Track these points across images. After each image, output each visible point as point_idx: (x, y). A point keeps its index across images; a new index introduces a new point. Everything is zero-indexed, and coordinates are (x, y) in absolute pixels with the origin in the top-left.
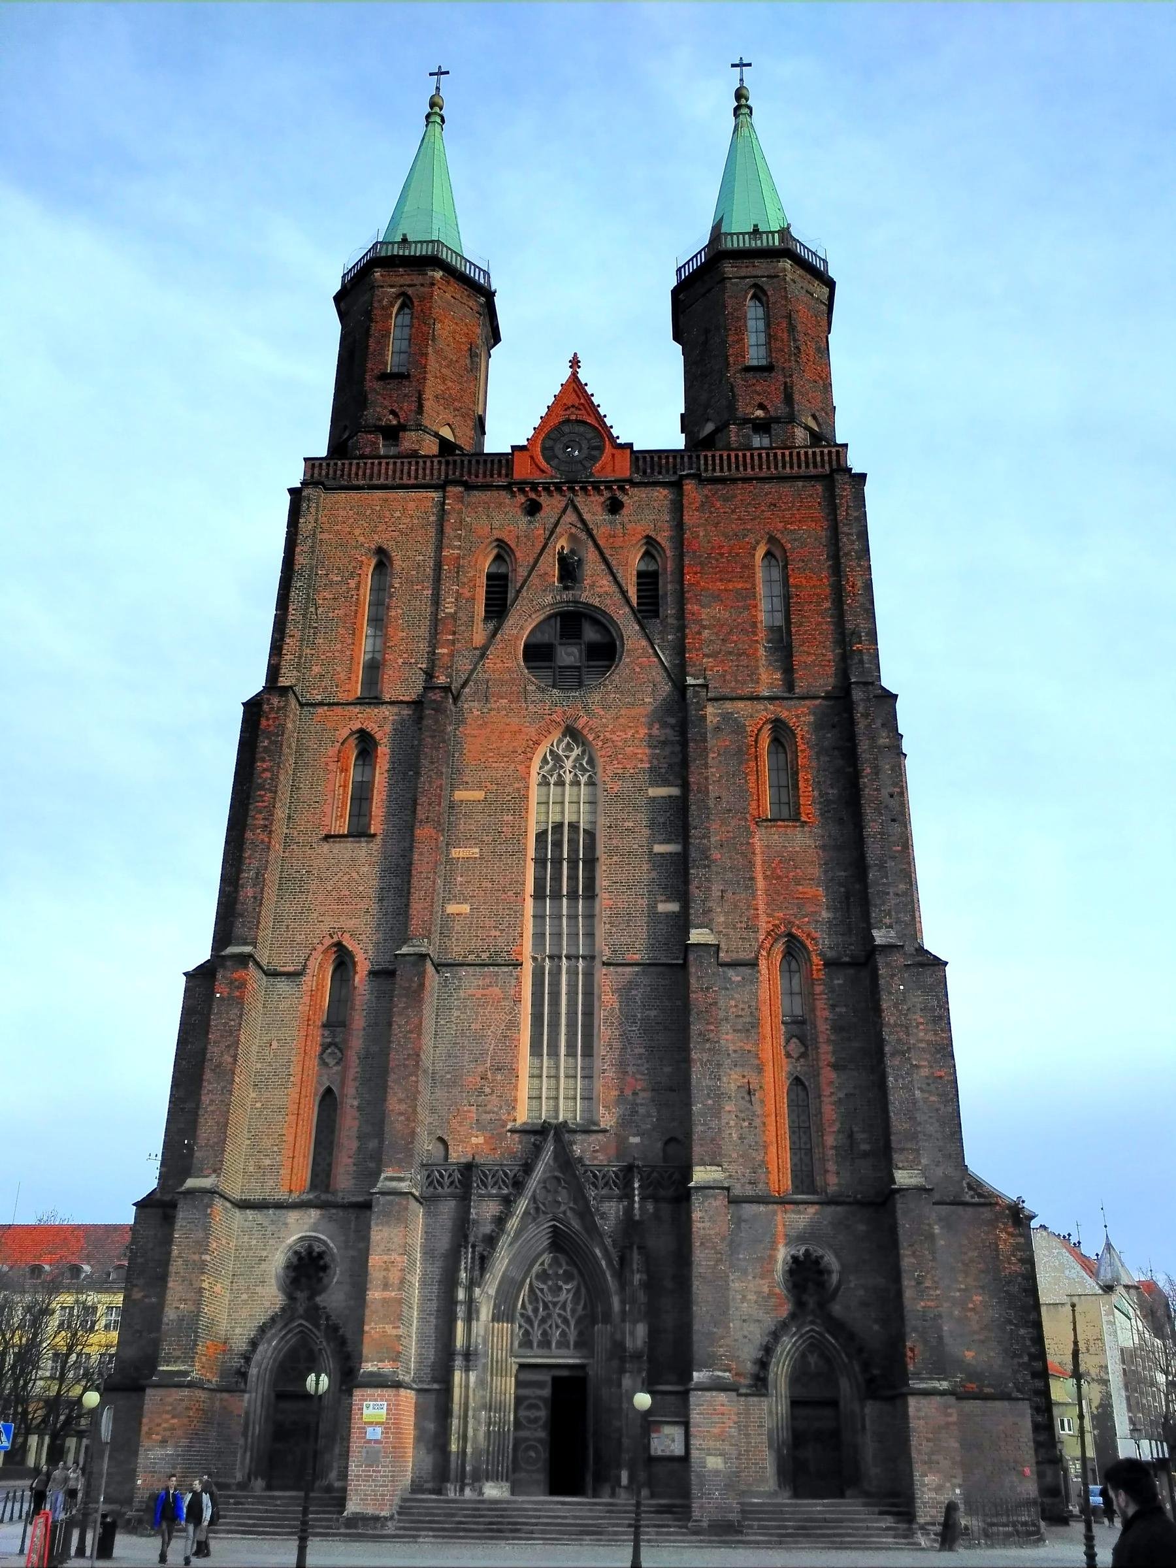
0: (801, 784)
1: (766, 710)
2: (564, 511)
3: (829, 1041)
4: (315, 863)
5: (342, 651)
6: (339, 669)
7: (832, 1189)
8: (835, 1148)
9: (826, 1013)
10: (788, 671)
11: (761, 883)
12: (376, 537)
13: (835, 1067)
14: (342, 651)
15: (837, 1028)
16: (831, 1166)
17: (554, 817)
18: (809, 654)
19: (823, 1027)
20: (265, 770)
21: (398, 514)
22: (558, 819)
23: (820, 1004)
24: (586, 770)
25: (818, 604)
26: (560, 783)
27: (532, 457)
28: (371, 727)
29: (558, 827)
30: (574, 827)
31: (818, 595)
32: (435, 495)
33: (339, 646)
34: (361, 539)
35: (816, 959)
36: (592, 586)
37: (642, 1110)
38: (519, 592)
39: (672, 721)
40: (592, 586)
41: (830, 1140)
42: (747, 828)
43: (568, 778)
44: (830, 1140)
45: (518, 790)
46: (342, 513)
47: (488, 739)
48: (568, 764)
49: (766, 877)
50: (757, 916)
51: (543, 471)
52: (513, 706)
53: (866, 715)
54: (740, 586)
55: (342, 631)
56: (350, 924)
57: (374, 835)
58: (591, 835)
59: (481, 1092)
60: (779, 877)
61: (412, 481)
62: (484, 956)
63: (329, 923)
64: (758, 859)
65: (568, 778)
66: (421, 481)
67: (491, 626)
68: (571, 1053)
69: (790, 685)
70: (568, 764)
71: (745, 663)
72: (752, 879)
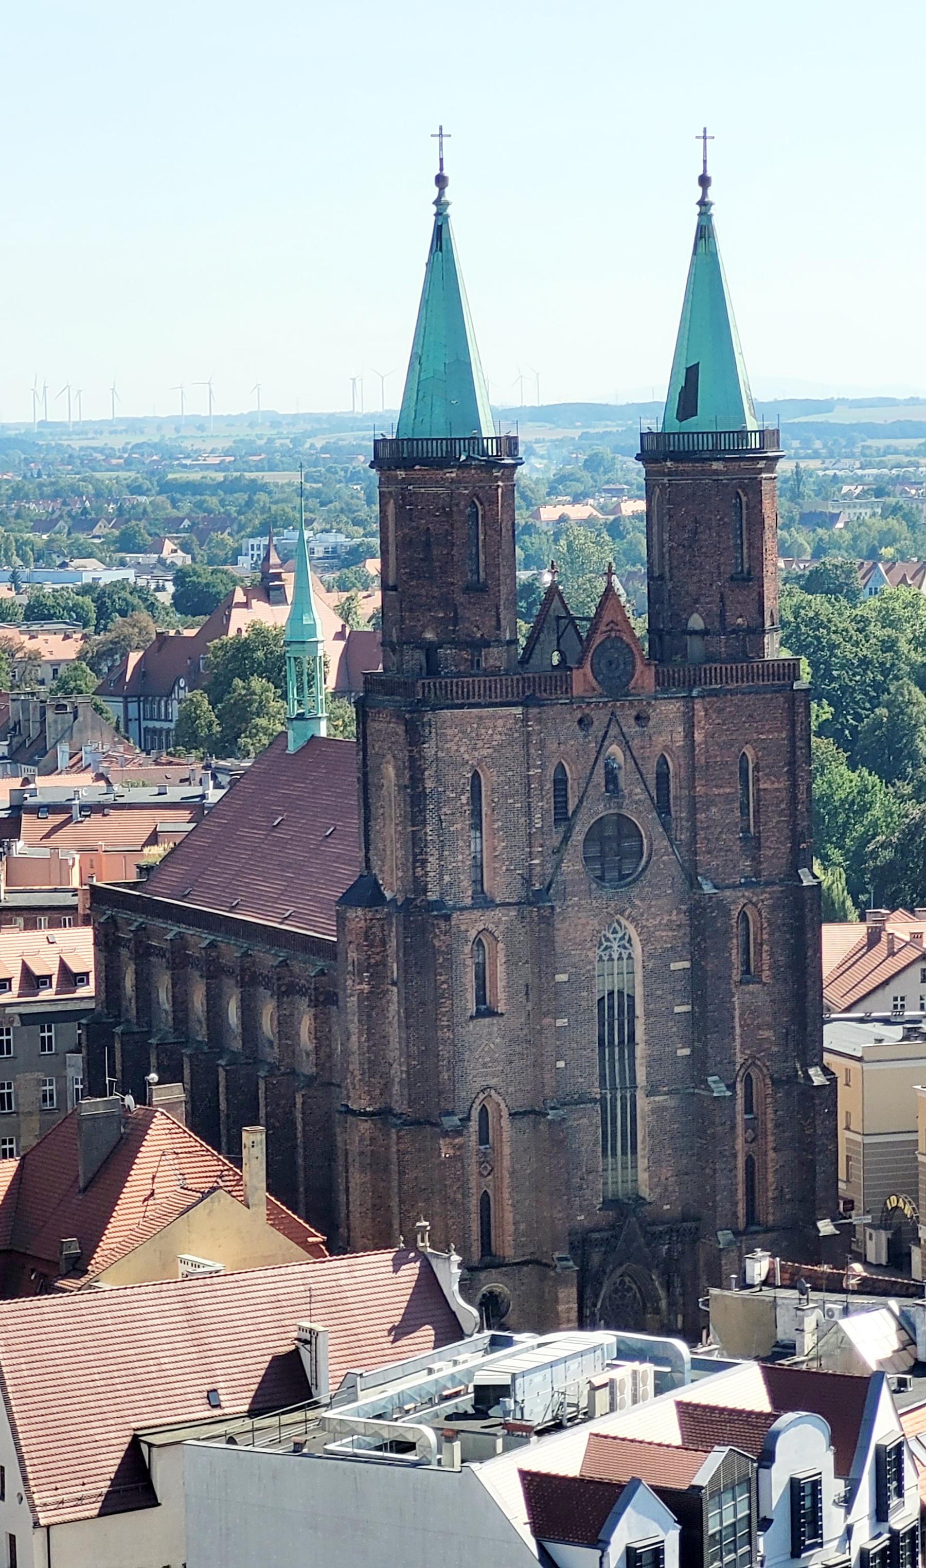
0: (764, 955)
1: (743, 896)
2: (608, 726)
3: (773, 1134)
4: (465, 1038)
5: (463, 862)
6: (462, 877)
7: (771, 1223)
8: (773, 1199)
9: (772, 1116)
10: (756, 860)
11: (738, 1031)
12: (476, 753)
13: (775, 1149)
14: (463, 862)
15: (776, 1126)
16: (771, 1210)
17: (608, 987)
18: (770, 848)
19: (770, 1125)
20: (443, 982)
21: (490, 732)
22: (610, 988)
23: (769, 1110)
24: (625, 948)
25: (778, 805)
26: (611, 959)
27: (585, 675)
28: (491, 927)
29: (611, 993)
30: (621, 993)
31: (777, 797)
32: (518, 711)
33: (460, 857)
34: (466, 756)
35: (768, 1081)
36: (630, 794)
37: (670, 1189)
38: (581, 802)
39: (683, 907)
40: (630, 794)
41: (770, 1194)
42: (730, 989)
43: (615, 956)
44: (770, 1194)
45: (589, 971)
46: (449, 732)
47: (567, 931)
48: (615, 945)
49: (741, 1026)
50: (735, 1054)
51: (594, 690)
52: (583, 902)
53: (811, 911)
54: (728, 790)
55: (461, 843)
56: (493, 1082)
57: (502, 1014)
58: (631, 998)
59: (581, 1188)
60: (748, 1025)
61: (498, 700)
62: (576, 1097)
63: (480, 1083)
64: (737, 1013)
65: (615, 956)
66: (505, 700)
67: (562, 829)
68: (624, 1153)
69: (757, 874)
70: (615, 945)
71: (730, 857)
72: (733, 1028)
